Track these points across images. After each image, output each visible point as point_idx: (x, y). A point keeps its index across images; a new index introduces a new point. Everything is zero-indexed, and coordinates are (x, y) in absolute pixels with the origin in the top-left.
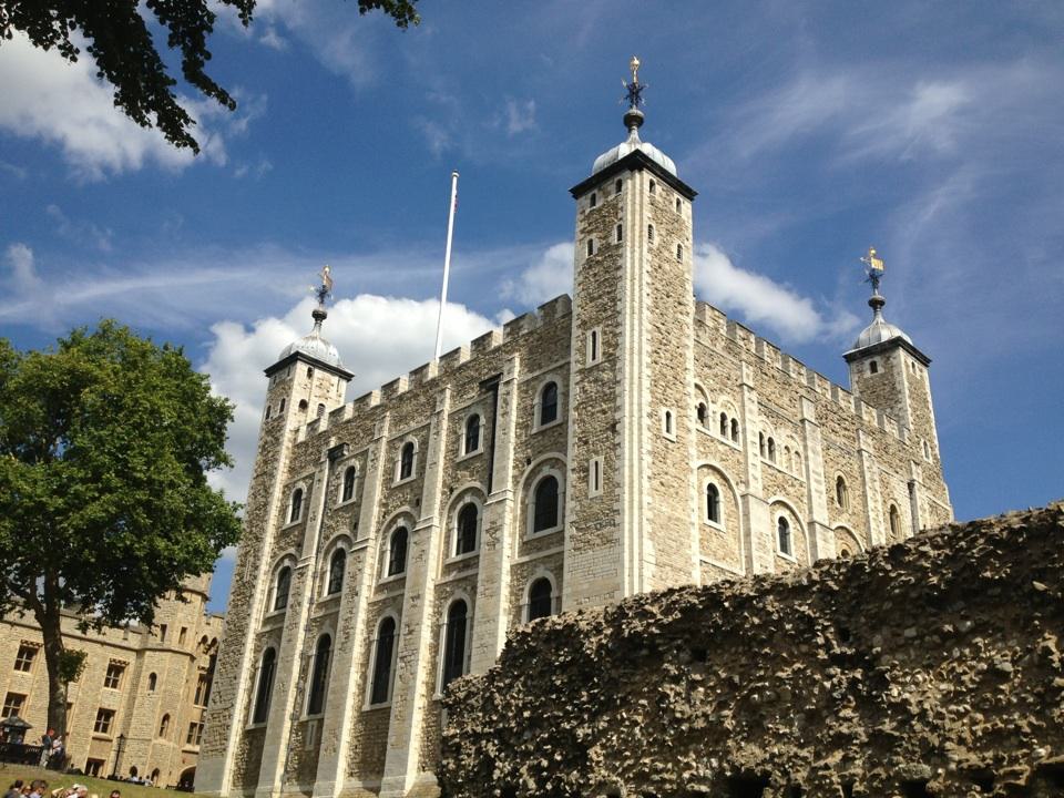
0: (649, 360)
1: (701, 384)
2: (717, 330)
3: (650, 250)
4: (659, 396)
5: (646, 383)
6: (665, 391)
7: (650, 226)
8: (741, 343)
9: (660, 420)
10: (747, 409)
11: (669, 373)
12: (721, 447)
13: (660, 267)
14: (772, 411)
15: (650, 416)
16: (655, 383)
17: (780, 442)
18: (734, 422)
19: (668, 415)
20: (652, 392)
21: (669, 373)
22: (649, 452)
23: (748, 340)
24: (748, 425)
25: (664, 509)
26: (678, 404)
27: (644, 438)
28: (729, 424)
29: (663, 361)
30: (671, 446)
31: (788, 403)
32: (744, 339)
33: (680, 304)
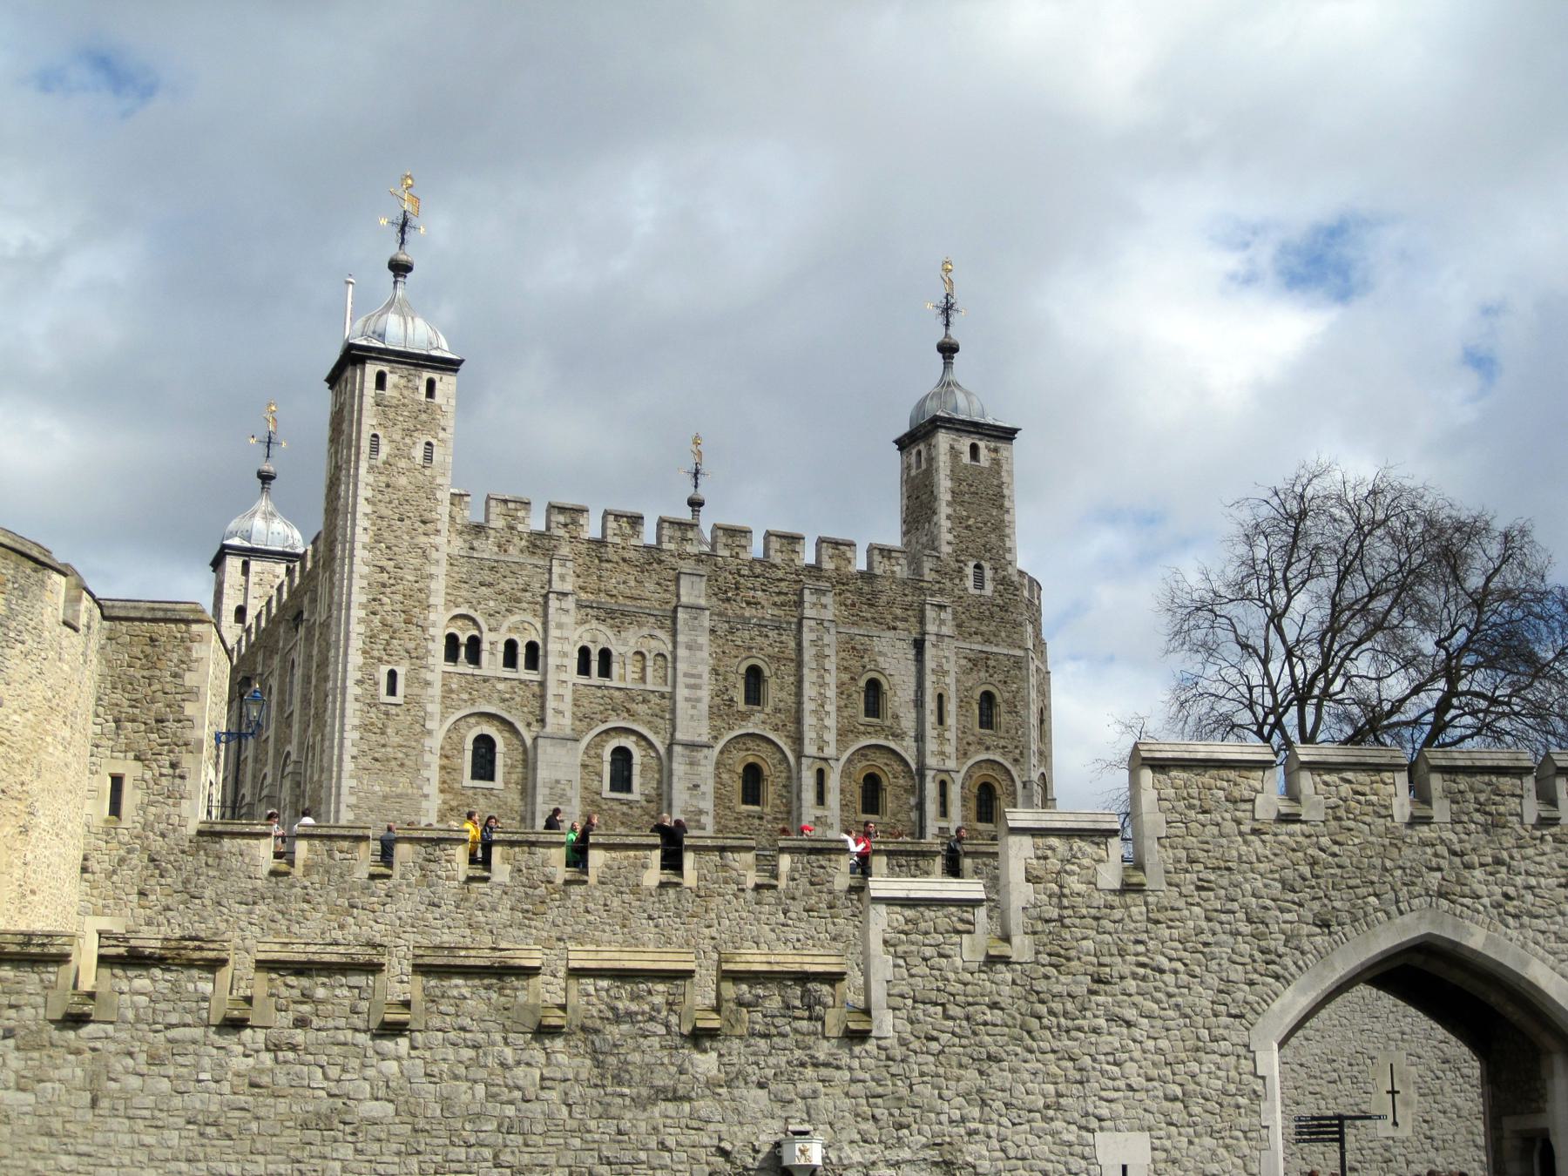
0: (363, 613)
1: (471, 613)
2: (512, 528)
3: (371, 469)
4: (376, 653)
7: (375, 436)
8: (561, 532)
9: (377, 684)
10: (552, 625)
11: (398, 621)
12: (501, 686)
13: (388, 486)
14: (613, 611)
15: (359, 682)
16: (372, 638)
17: (622, 649)
19: (392, 675)
20: (364, 652)
21: (398, 621)
22: (355, 728)
23: (574, 522)
24: (553, 647)
25: (377, 788)
26: (417, 657)
27: (349, 712)
29: (388, 608)
30: (393, 710)
32: (566, 525)
33: (424, 522)
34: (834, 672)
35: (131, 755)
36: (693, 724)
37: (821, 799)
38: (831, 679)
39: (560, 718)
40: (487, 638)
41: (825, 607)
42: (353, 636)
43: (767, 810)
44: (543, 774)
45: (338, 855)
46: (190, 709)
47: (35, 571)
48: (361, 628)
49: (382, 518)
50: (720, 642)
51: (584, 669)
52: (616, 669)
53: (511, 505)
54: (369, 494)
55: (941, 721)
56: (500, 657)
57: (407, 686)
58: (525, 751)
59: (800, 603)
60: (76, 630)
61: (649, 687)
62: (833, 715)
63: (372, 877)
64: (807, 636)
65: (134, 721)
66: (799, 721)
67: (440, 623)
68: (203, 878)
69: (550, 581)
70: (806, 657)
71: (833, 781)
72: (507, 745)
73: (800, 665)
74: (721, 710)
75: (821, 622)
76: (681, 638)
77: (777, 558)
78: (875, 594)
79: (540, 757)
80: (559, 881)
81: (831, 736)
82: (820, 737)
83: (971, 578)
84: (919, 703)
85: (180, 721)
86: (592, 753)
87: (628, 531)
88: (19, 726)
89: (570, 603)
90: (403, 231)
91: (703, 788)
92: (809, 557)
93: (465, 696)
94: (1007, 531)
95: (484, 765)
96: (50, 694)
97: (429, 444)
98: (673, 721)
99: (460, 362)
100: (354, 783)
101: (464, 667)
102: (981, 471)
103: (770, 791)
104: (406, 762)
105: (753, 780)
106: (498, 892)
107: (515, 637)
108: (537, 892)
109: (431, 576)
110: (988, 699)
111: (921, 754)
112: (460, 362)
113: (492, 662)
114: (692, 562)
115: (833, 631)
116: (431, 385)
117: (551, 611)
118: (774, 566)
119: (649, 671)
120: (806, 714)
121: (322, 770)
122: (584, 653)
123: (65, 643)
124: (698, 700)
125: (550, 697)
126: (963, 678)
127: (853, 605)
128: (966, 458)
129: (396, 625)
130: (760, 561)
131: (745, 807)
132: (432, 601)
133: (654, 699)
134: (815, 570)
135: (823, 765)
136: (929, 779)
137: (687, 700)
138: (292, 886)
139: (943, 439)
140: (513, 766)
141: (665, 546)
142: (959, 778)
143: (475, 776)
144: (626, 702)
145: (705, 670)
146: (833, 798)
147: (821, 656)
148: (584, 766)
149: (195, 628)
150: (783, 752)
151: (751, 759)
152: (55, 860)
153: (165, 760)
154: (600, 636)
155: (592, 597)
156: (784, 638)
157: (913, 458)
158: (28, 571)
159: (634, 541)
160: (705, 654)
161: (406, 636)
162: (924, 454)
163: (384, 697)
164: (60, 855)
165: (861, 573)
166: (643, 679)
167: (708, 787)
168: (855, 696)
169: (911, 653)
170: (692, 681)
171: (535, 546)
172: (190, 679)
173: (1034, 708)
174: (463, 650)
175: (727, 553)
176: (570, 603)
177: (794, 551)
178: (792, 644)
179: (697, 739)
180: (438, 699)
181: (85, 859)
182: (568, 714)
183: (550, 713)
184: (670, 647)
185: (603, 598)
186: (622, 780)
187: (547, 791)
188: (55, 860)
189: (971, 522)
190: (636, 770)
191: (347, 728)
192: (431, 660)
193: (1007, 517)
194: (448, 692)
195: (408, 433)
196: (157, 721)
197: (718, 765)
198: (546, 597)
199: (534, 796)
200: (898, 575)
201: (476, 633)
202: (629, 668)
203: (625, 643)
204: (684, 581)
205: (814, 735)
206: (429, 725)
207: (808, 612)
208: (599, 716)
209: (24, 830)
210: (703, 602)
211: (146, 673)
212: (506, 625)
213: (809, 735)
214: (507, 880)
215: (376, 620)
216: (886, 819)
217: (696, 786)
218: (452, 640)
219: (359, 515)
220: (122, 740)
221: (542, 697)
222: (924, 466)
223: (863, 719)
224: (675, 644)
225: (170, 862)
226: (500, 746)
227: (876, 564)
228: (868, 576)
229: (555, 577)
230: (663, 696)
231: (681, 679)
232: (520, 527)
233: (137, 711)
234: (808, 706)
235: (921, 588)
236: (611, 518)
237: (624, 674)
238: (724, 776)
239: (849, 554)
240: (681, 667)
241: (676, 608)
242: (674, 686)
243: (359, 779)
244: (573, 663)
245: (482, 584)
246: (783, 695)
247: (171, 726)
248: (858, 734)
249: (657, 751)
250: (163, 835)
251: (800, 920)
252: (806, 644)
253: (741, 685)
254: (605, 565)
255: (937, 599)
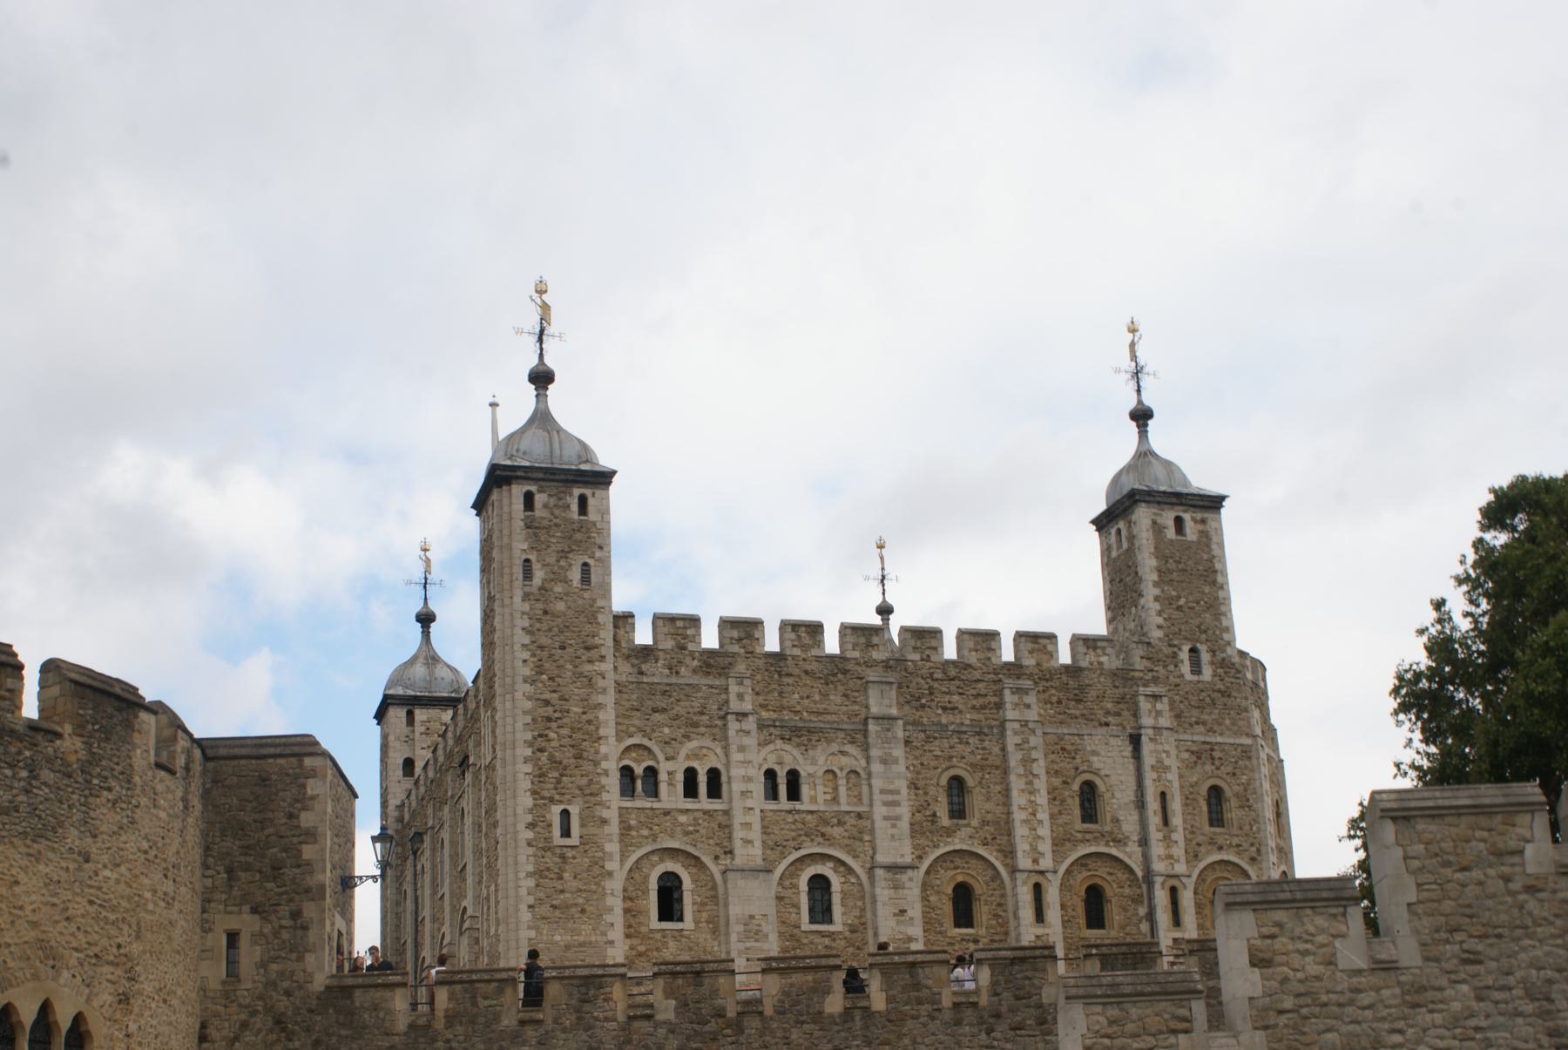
0: (529, 752)
1: (646, 742)
2: (683, 648)
3: (526, 597)
4: (546, 794)
5: (525, 784)
6: (559, 782)
8: (735, 648)
9: (550, 825)
10: (734, 747)
11: (567, 756)
12: (683, 819)
13: (545, 612)
15: (531, 826)
16: (541, 776)
17: (811, 769)
18: (714, 775)
19: (565, 814)
20: (534, 793)
21: (567, 756)
23: (750, 636)
24: (736, 772)
26: (591, 793)
27: (522, 858)
28: (702, 780)
29: (555, 744)
31: (839, 700)
32: (740, 640)
33: (588, 648)
34: (1044, 777)
35: (246, 908)
36: (894, 845)
37: (1040, 916)
38: (1041, 784)
39: (750, 851)
40: (664, 768)
41: (1028, 706)
42: (521, 776)
43: (983, 932)
44: (736, 910)
45: (483, 1003)
46: (308, 852)
47: (119, 710)
48: (528, 768)
49: (541, 648)
50: (918, 753)
51: (772, 794)
52: (805, 790)
53: (680, 624)
54: (526, 623)
55: (1166, 822)
56: (680, 788)
57: (582, 826)
58: (714, 887)
59: (999, 706)
60: (172, 772)
61: (845, 808)
62: (1047, 823)
63: (522, 1023)
64: (1012, 740)
65: (246, 870)
66: (1010, 833)
67: (610, 755)
68: (334, 1040)
69: (727, 702)
70: (1012, 763)
71: (1052, 895)
72: (694, 881)
73: (1006, 772)
74: (923, 828)
75: (1025, 723)
76: (874, 752)
77: (973, 658)
78: (1082, 689)
79: (731, 891)
80: (731, 1013)
81: (1046, 847)
82: (1034, 849)
83: (1187, 663)
84: (1140, 804)
85: (299, 866)
86: (787, 883)
87: (807, 640)
88: (112, 883)
89: (750, 723)
90: (540, 340)
91: (910, 913)
92: (1007, 654)
93: (645, 832)
94: (1223, 608)
95: (669, 905)
96: (145, 845)
97: (585, 564)
98: (872, 842)
99: (614, 473)
100: (532, 934)
101: (642, 803)
102: (1188, 546)
103: (982, 912)
104: (588, 908)
105: (963, 900)
106: (662, 1032)
107: (695, 764)
108: (707, 1028)
109: (599, 706)
110: (1216, 794)
111: (1146, 858)
112: (614, 473)
113: (671, 795)
114: (880, 669)
115: (1039, 732)
116: (583, 501)
117: (731, 733)
118: (969, 666)
119: (842, 790)
120: (1017, 824)
121: (498, 924)
122: (770, 775)
123: (159, 787)
124: (898, 818)
125: (736, 826)
126: (1187, 773)
127: (1059, 702)
128: (1171, 533)
129: (565, 762)
130: (953, 662)
131: (958, 931)
132: (602, 732)
133: (851, 821)
134: (1014, 669)
135: (1040, 879)
136: (1157, 886)
137: (886, 818)
138: (434, 1040)
139: (1143, 516)
140: (703, 904)
141: (849, 655)
142: (1190, 883)
143: (661, 919)
144: (819, 826)
145: (902, 785)
146: (1053, 914)
147: (1027, 761)
148: (779, 898)
149: (308, 762)
150: (995, 868)
151: (960, 878)
152: (165, 1029)
153: (284, 910)
154: (787, 756)
155: (774, 716)
156: (986, 744)
157: (1113, 538)
158: (110, 710)
159: (814, 652)
160: (901, 768)
161: (576, 772)
162: (1124, 533)
163: (558, 840)
164: (170, 1024)
165: (1066, 667)
166: (835, 800)
167: (916, 911)
168: (1069, 801)
169: (1128, 750)
170: (890, 798)
171: (709, 666)
172: (306, 820)
173: (1268, 801)
174: (639, 783)
175: (917, 657)
176: (750, 723)
177: (990, 649)
178: (996, 750)
179: (900, 860)
180: (616, 838)
181: (203, 1026)
182: (758, 843)
183: (738, 843)
184: (863, 763)
185: (787, 715)
186: (821, 911)
187: (741, 928)
188: (165, 1029)
189: (1182, 602)
190: (836, 899)
191: (522, 875)
192: (605, 796)
193: (1221, 594)
194: (626, 829)
195: (564, 554)
196: (274, 868)
197: (925, 886)
198: (724, 718)
199: (727, 934)
200: (1106, 666)
201: (651, 763)
202: (820, 789)
203: (814, 762)
204: (873, 693)
205: (1027, 847)
206: (609, 866)
207: (1010, 714)
208: (792, 844)
209: (124, 999)
210: (894, 711)
211: (257, 816)
212: (683, 752)
213: (1022, 846)
214: (671, 1016)
215: (544, 757)
216: (1113, 933)
217: (903, 912)
218: (627, 772)
219: (517, 647)
220: (236, 892)
221: (726, 827)
222: (1125, 545)
223: (1079, 826)
224: (868, 759)
225: (296, 1023)
226: (687, 883)
227: (1079, 657)
228: (1073, 670)
229: (732, 697)
230: (859, 816)
231: (877, 797)
232: (691, 647)
233: (250, 859)
234: (1018, 816)
235: (1133, 678)
236: (789, 629)
237: (814, 796)
238: (933, 898)
239: (1050, 648)
240: (877, 783)
241: (866, 719)
242: (871, 805)
243: (537, 928)
244: (758, 787)
245: (655, 710)
246: (988, 806)
247: (289, 873)
248: (1076, 843)
249: (858, 877)
250: (288, 993)
251: (1007, 1040)
252: (1010, 748)
253: (943, 799)
254: (785, 680)
255: (1151, 690)
